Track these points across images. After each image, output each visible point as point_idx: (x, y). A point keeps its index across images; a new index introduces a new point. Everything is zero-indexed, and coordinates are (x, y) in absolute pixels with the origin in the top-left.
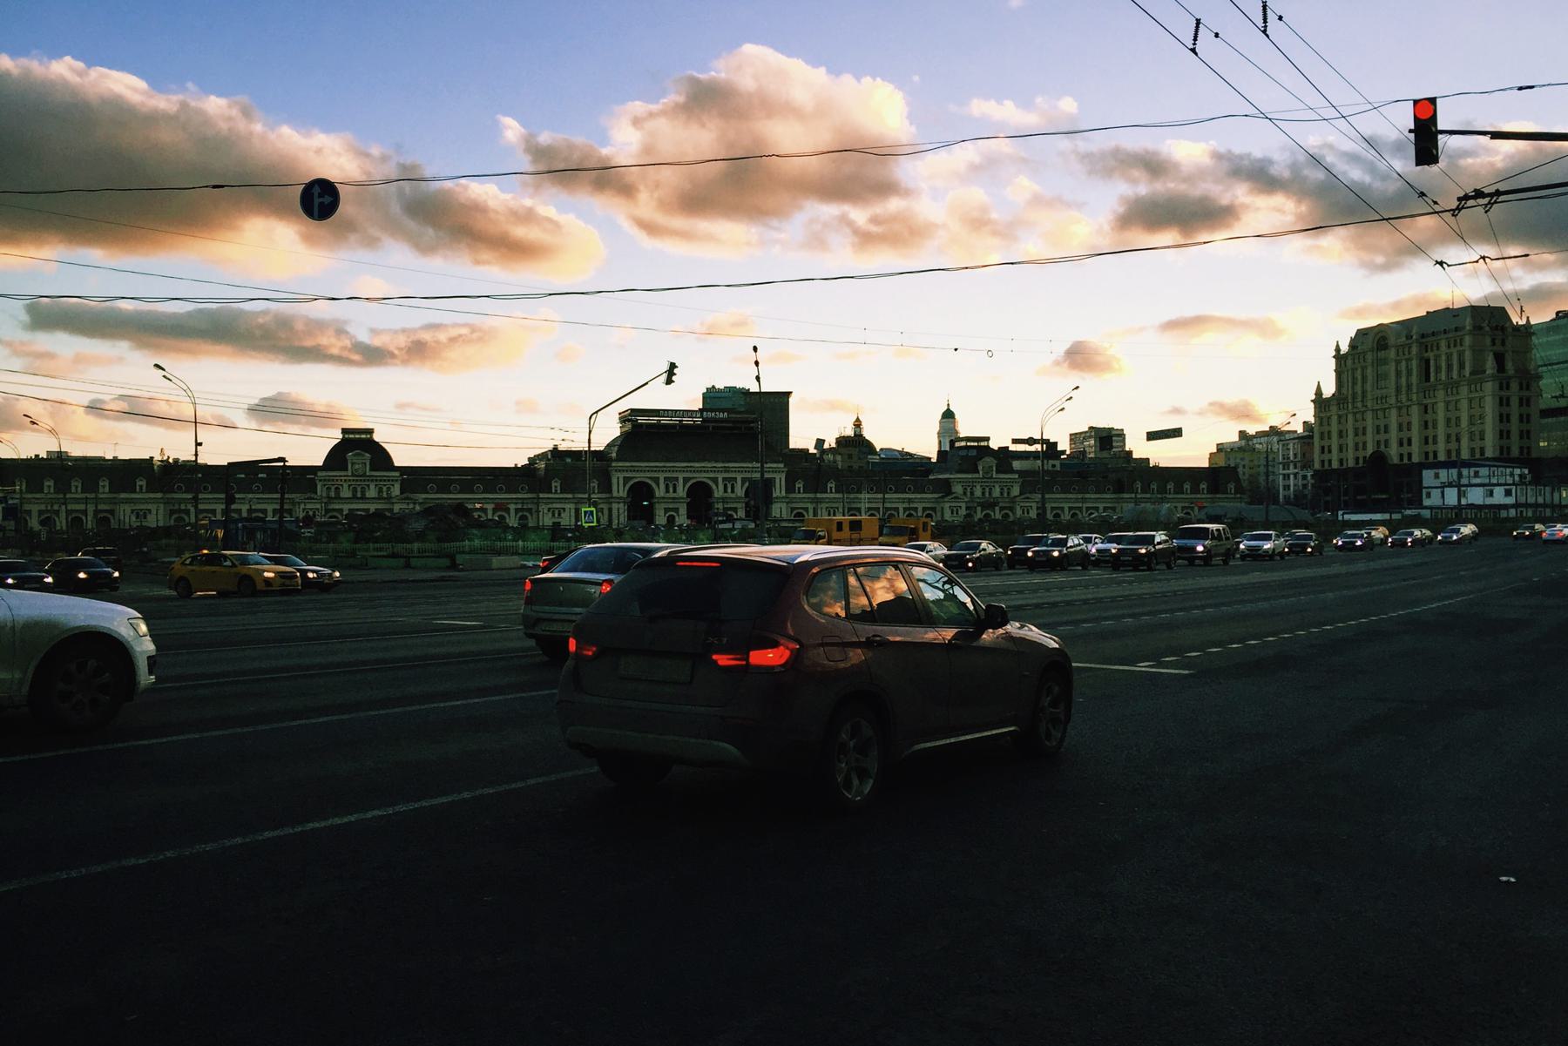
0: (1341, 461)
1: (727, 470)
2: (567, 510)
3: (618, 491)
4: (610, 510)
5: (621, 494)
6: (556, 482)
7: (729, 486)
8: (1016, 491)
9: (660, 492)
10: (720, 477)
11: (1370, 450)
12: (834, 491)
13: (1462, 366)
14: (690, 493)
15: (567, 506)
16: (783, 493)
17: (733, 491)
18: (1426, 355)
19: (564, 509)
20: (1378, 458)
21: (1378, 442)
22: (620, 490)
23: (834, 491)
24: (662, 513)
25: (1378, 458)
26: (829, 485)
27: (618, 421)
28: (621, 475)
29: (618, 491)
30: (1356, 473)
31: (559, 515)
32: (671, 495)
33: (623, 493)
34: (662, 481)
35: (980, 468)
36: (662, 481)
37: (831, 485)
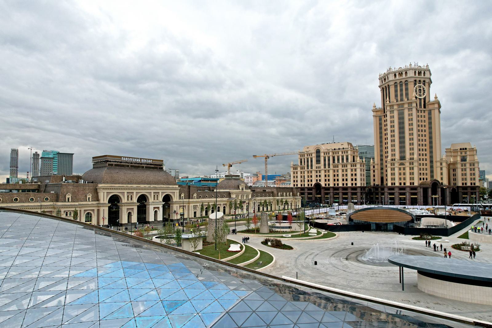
0: (301, 185)
1: (155, 188)
3: (104, 201)
4: (98, 210)
6: (69, 195)
7: (156, 196)
8: (250, 197)
11: (314, 182)
12: (196, 198)
13: (347, 159)
14: (139, 200)
16: (178, 200)
18: (334, 155)
20: (318, 186)
21: (317, 180)
22: (104, 198)
23: (196, 198)
24: (126, 210)
25: (318, 186)
26: (194, 195)
27: (92, 161)
28: (106, 191)
29: (104, 201)
30: (309, 189)
32: (130, 201)
33: (106, 201)
34: (126, 194)
35: (241, 188)
36: (126, 194)
37: (195, 195)
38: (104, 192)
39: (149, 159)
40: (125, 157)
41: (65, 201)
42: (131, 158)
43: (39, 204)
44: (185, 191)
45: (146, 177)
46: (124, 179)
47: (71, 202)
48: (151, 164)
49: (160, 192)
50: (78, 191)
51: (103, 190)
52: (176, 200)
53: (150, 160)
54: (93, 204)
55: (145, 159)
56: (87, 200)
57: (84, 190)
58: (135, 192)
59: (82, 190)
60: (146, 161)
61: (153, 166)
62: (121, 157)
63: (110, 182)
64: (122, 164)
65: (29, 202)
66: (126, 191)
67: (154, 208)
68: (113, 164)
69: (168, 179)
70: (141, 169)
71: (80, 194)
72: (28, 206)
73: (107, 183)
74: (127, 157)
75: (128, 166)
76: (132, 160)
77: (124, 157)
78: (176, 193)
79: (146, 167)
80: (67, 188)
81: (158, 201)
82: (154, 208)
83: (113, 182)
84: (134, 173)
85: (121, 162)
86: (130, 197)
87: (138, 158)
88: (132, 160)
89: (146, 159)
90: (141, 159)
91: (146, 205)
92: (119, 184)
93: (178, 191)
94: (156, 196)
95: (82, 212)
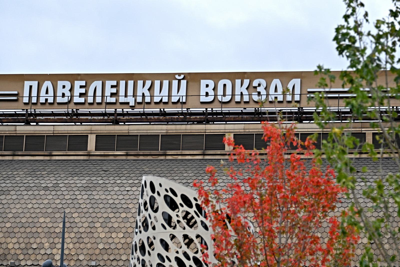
42: (104, 77)
55: (232, 76)
84: (86, 188)
87: (171, 76)
89: (242, 76)
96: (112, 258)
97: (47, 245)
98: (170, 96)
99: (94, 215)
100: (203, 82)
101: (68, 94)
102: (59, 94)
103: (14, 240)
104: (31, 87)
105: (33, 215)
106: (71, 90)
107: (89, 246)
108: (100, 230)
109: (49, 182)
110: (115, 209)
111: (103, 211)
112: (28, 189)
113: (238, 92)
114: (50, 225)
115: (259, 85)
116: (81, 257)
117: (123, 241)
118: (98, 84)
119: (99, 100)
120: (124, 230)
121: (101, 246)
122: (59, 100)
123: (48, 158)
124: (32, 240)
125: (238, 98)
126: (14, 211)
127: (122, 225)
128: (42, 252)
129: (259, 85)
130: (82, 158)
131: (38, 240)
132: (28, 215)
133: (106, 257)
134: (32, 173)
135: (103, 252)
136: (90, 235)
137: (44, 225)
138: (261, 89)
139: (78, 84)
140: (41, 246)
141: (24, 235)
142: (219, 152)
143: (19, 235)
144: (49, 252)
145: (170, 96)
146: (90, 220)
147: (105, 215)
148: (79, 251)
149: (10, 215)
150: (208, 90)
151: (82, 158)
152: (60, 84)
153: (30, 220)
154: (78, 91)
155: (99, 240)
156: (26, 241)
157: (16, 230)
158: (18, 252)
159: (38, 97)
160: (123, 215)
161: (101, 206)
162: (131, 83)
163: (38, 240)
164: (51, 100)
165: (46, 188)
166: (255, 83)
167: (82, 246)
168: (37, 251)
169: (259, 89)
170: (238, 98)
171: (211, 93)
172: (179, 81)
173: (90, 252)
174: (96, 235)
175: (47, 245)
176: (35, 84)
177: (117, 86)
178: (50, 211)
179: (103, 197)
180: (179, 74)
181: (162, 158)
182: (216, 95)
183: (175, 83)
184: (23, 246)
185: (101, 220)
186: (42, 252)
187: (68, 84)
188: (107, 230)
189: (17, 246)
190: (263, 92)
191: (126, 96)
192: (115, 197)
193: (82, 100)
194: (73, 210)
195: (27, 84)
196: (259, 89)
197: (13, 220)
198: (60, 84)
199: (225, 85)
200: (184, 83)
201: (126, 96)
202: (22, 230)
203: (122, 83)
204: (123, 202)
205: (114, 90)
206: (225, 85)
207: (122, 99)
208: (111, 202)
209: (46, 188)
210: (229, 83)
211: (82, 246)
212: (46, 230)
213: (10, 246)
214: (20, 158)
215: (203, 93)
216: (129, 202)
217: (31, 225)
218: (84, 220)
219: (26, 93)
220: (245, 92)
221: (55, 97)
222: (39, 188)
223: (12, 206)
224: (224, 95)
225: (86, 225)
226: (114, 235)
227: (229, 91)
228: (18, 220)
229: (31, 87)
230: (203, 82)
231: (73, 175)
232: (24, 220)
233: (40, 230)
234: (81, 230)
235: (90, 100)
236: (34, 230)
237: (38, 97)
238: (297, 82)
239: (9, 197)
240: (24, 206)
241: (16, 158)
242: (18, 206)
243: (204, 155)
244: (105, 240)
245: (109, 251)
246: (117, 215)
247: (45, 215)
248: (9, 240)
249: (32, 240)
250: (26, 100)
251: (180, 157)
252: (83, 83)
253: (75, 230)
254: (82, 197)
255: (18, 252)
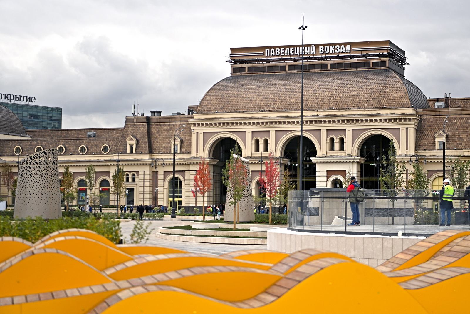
2: (141, 174)
3: (197, 152)
5: (200, 154)
6: (131, 139)
9: (248, 150)
10: (324, 128)
15: (140, 169)
17: (342, 148)
19: (137, 172)
28: (201, 130)
29: (197, 152)
31: (134, 180)
38: (197, 133)
39: (340, 44)
40: (275, 47)
41: (125, 153)
42: (290, 47)
43: (115, 157)
44: (456, 123)
45: (314, 91)
46: (251, 100)
47: (137, 153)
48: (351, 57)
49: (349, 128)
50: (158, 131)
51: (195, 128)
52: (404, 151)
53: (345, 44)
54: (182, 159)
55: (329, 45)
56: (171, 151)
57: (171, 129)
58: (273, 129)
59: (167, 130)
60: (332, 49)
61: (355, 60)
62: (264, 48)
63: (214, 110)
64: (271, 64)
65: (79, 154)
66: (249, 130)
67: (330, 173)
68: (245, 68)
69: (385, 92)
70: (318, 71)
71: (161, 137)
72: (98, 161)
73: (209, 112)
74: (280, 47)
75: (282, 68)
76: (291, 51)
77: (270, 48)
78: (403, 133)
79: (333, 66)
80: (135, 125)
81: (343, 155)
82: (330, 173)
83: (223, 108)
84: (284, 85)
85: (268, 61)
86: (261, 142)
88: (291, 51)
90: (317, 46)
91: (315, 164)
92: (235, 111)
93: (412, 127)
94: (337, 141)
95: (161, 177)
96: (291, 107)
97: (272, 104)
98: (310, 52)
99: (286, 94)
100: (320, 47)
101: (279, 53)
102: (276, 53)
103: (263, 103)
104: (267, 51)
105: (268, 95)
106: (280, 51)
107: (285, 104)
108: (288, 99)
109: (273, 83)
110: (292, 91)
111: (289, 92)
112: (267, 85)
113: (331, 50)
114: (273, 98)
115: (337, 47)
116: (282, 108)
117: (295, 102)
118: (288, 49)
119: (288, 54)
120: (295, 98)
121: (288, 104)
122: (276, 55)
123: (274, 73)
124: (268, 103)
125: (331, 52)
126: (263, 93)
127: (294, 97)
128: (271, 106)
129: (337, 47)
130: (284, 73)
131: (270, 103)
132: (267, 95)
133: (290, 107)
134: (268, 80)
135: (289, 106)
136: (285, 100)
137: (271, 98)
138: (338, 49)
139: (282, 49)
140: (271, 105)
141: (266, 101)
142: (325, 70)
143: (264, 101)
144: (273, 106)
145: (310, 52)
146: (285, 95)
147: (289, 94)
148: (282, 106)
149: (261, 95)
150: (321, 49)
151: (284, 73)
152: (276, 49)
153: (267, 96)
154: (282, 51)
155: (287, 102)
156: (266, 103)
157: (263, 100)
158: (264, 106)
159: (270, 54)
160: (295, 94)
161: (288, 91)
162: (298, 48)
163: (270, 103)
164: (274, 55)
165: (272, 85)
166: (336, 47)
167: (283, 104)
168: (270, 106)
169: (337, 49)
170: (331, 52)
171: (323, 51)
172: (313, 47)
173: (285, 106)
174: (287, 100)
175: (272, 104)
176: (269, 49)
177: (294, 49)
178: (273, 93)
179: (289, 88)
180: (313, 45)
181: (309, 72)
182: (324, 51)
183: (311, 48)
184: (265, 104)
185: (288, 95)
186: (271, 106)
187: (279, 49)
188: (290, 98)
189: (264, 105)
190: (339, 50)
191: (297, 52)
192: (293, 87)
193: (283, 54)
194: (280, 93)
195: (266, 50)
196: (337, 49)
197: (262, 96)
198: (276, 49)
199: (327, 48)
200: (314, 47)
201: (297, 52)
202: (265, 99)
203: (295, 48)
204: (295, 89)
205: (293, 51)
206: (327, 48)
207: (295, 54)
208: (291, 89)
209: (272, 85)
210: (328, 47)
211: (283, 104)
212: (272, 99)
213: (262, 105)
214: (266, 74)
215: (320, 51)
216: (297, 89)
217: (268, 98)
218: (283, 96)
219: (266, 53)
220: (333, 50)
221: (275, 54)
222: (270, 85)
223: (262, 92)
224: (327, 51)
225: (284, 97)
226: (292, 100)
227: (328, 50)
228: (264, 96)
229: (267, 51)
230: (320, 47)
231: (281, 80)
232: (265, 96)
233: (270, 99)
234: (282, 99)
235: (286, 54)
236: (268, 99)
237: (270, 54)
238: (349, 46)
239: (261, 89)
240: (266, 91)
241: (264, 74)
242: (264, 92)
243: (321, 71)
244: (289, 102)
245: (291, 105)
246: (293, 94)
247: (272, 94)
248: (261, 103)
249: (268, 103)
250: (266, 55)
251: (314, 72)
252: (283, 49)
253: (281, 99)
254: (283, 88)
255: (264, 106)
